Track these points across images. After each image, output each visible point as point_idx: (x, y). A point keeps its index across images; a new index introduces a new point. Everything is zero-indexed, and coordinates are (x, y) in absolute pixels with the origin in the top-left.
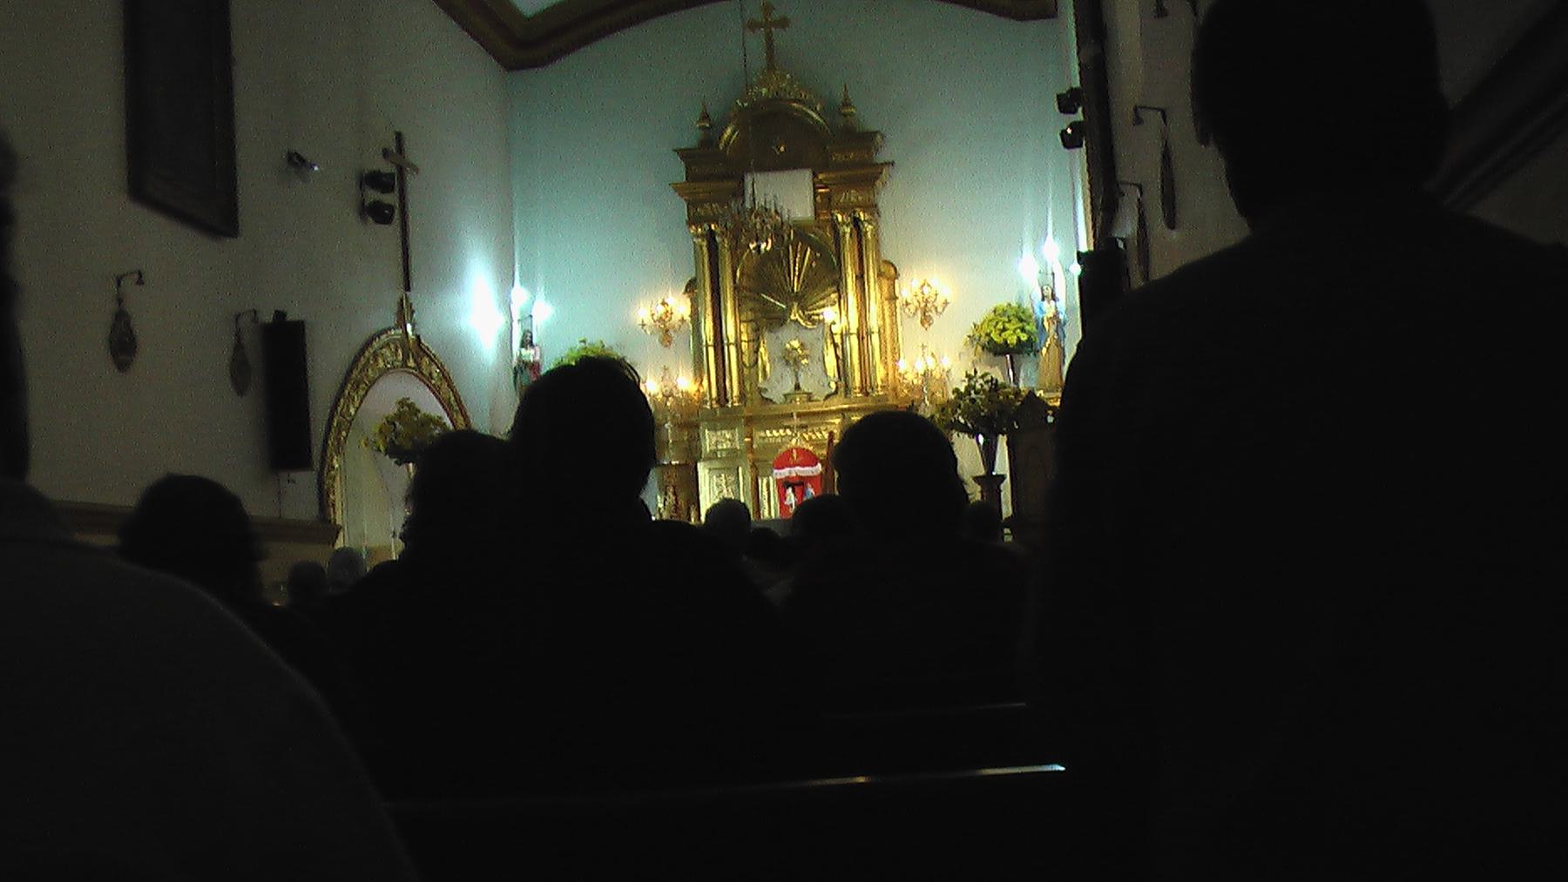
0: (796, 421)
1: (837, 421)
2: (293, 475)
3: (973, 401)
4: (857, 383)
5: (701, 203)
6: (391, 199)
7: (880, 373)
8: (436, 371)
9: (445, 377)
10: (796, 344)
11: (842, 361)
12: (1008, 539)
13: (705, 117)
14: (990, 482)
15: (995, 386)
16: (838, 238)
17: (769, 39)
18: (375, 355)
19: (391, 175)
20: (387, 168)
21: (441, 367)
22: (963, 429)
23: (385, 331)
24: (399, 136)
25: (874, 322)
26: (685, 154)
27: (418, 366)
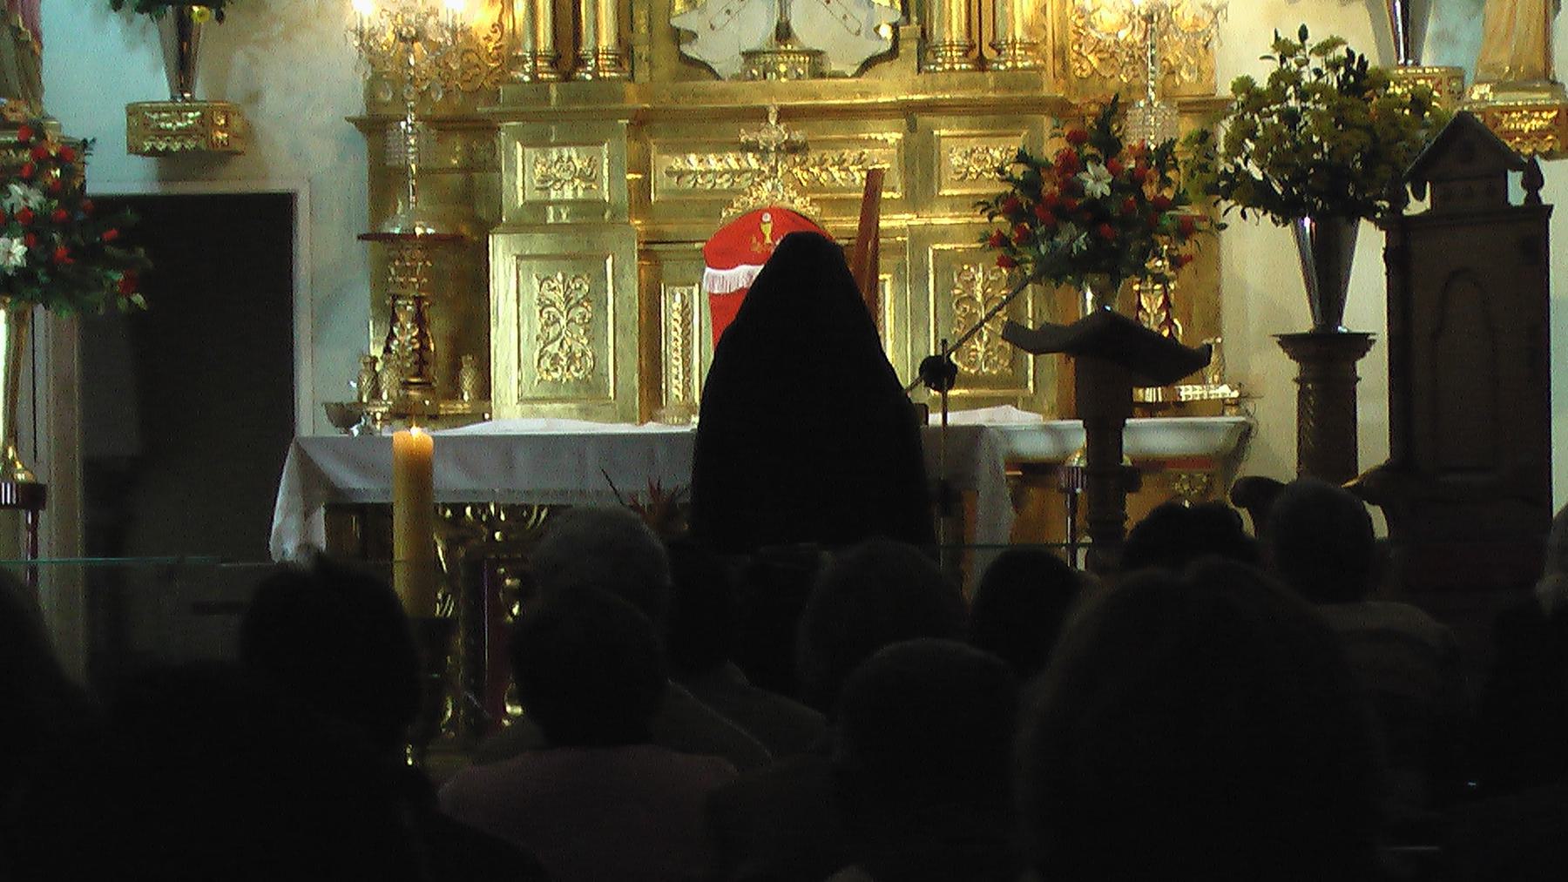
1: (894, 137)
3: (1291, 118)
4: (954, 30)
12: (1380, 526)
14: (1325, 355)
15: (1359, 80)
22: (1258, 197)
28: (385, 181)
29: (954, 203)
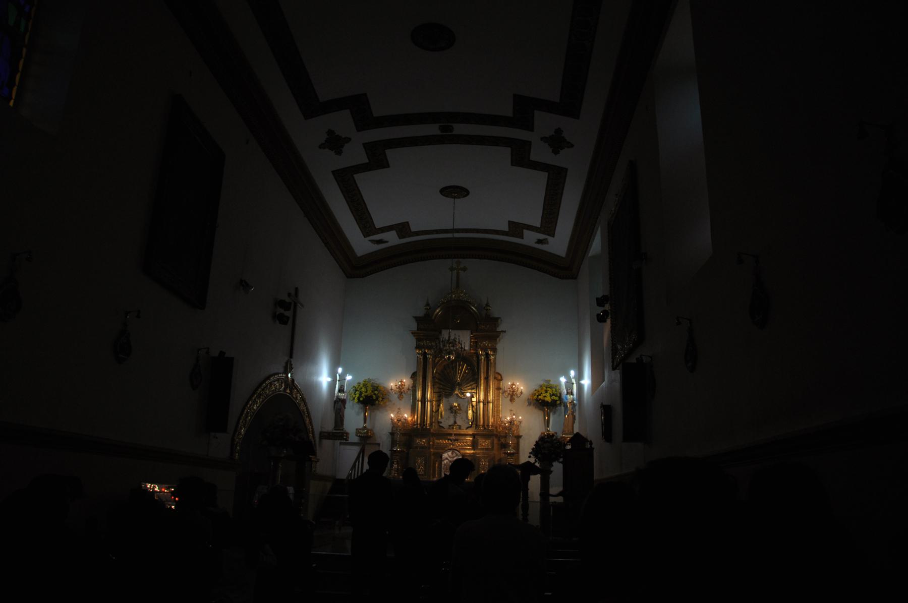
0: (453, 437)
4: (481, 423)
6: (288, 314)
7: (491, 420)
8: (299, 397)
9: (303, 400)
10: (456, 404)
11: (475, 413)
13: (428, 305)
16: (478, 361)
17: (458, 274)
18: (271, 384)
19: (290, 303)
20: (288, 300)
21: (302, 395)
23: (278, 374)
24: (297, 289)
25: (491, 398)
26: (417, 319)
27: (291, 393)
28: (394, 443)
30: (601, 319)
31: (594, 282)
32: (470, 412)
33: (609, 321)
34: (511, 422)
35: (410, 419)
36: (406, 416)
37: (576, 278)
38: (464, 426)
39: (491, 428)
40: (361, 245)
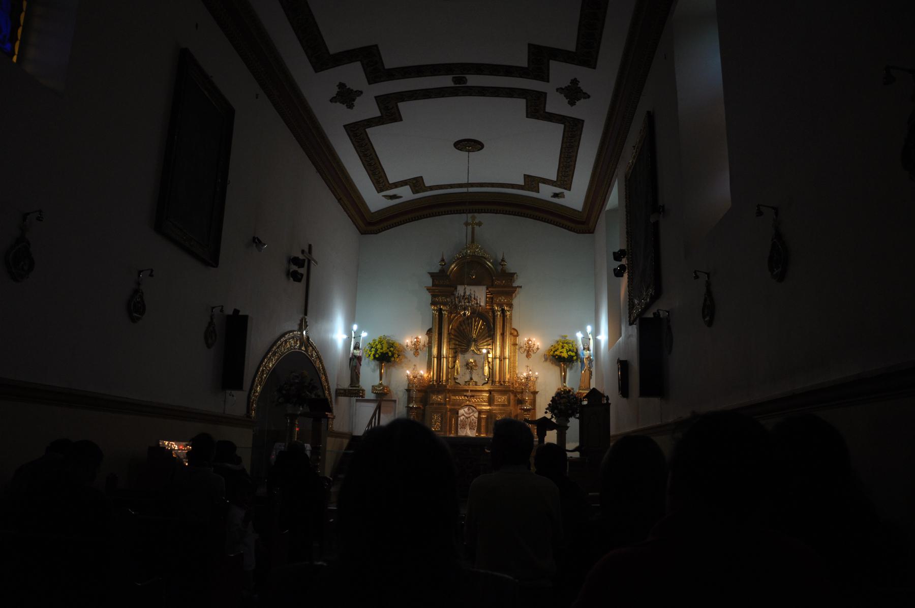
0: (469, 394)
2: (233, 392)
4: (497, 379)
5: (438, 296)
6: (303, 271)
7: (508, 376)
8: (314, 354)
9: (319, 357)
11: (492, 370)
13: (443, 260)
16: (494, 317)
17: (473, 229)
18: (286, 341)
20: (301, 257)
24: (310, 246)
25: (507, 354)
26: (432, 275)
27: (306, 351)
28: (410, 399)
29: (497, 405)
30: (618, 273)
31: (611, 236)
32: (486, 369)
33: (626, 275)
34: (527, 378)
35: (426, 375)
36: (423, 372)
37: (593, 233)
38: (480, 382)
39: (507, 384)
40: (375, 200)
